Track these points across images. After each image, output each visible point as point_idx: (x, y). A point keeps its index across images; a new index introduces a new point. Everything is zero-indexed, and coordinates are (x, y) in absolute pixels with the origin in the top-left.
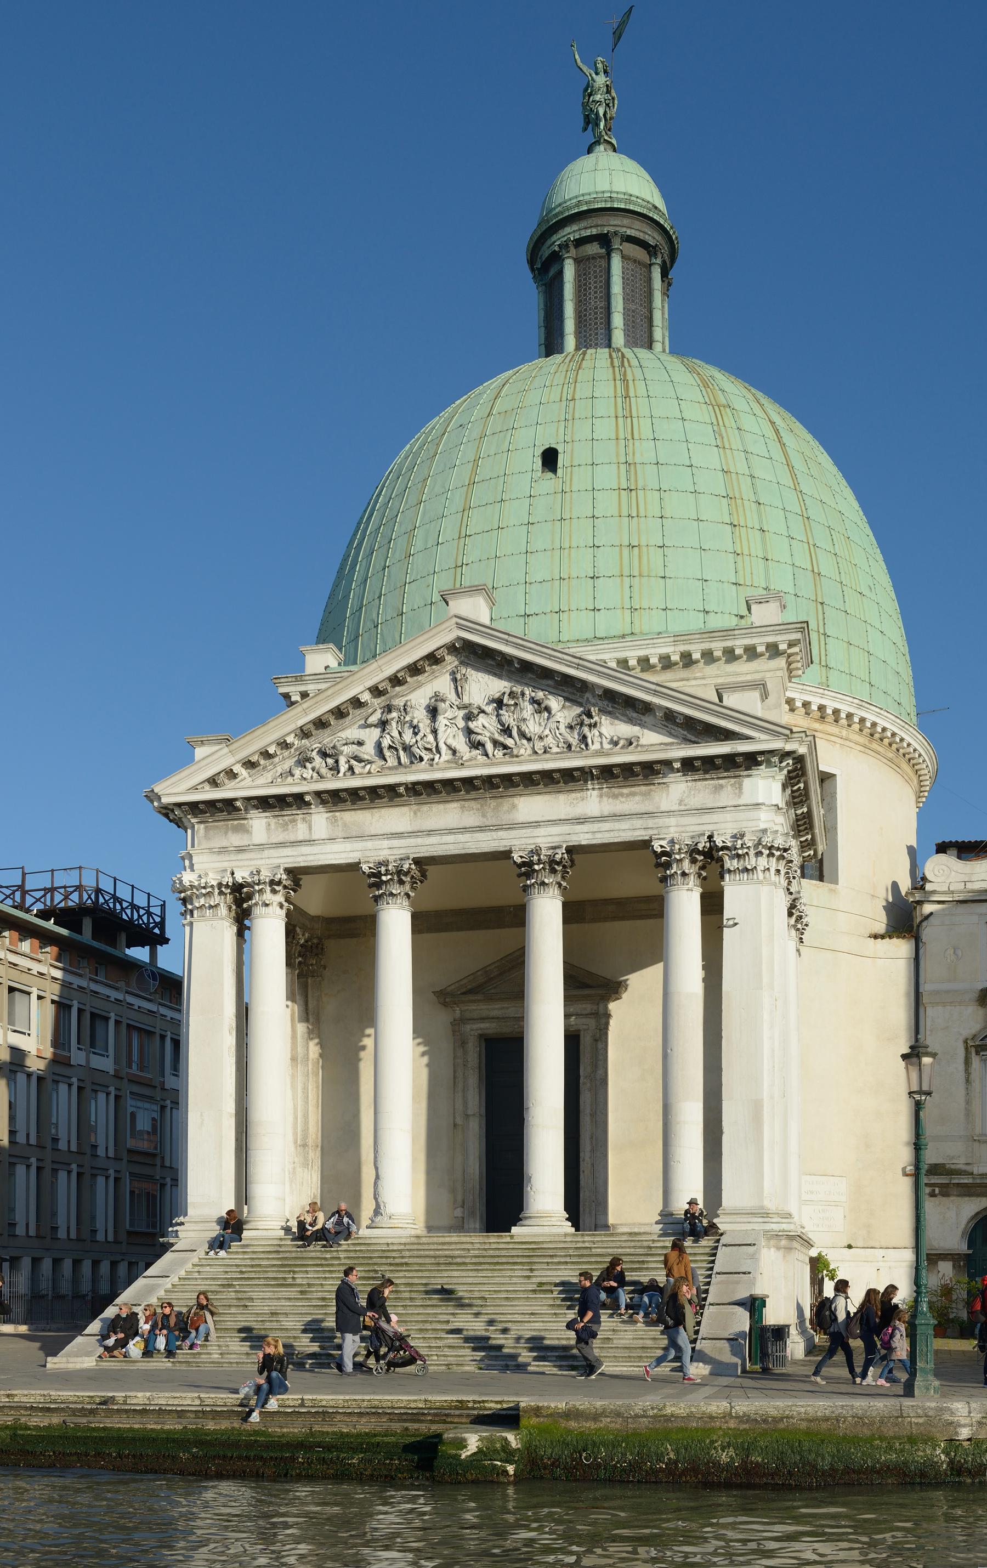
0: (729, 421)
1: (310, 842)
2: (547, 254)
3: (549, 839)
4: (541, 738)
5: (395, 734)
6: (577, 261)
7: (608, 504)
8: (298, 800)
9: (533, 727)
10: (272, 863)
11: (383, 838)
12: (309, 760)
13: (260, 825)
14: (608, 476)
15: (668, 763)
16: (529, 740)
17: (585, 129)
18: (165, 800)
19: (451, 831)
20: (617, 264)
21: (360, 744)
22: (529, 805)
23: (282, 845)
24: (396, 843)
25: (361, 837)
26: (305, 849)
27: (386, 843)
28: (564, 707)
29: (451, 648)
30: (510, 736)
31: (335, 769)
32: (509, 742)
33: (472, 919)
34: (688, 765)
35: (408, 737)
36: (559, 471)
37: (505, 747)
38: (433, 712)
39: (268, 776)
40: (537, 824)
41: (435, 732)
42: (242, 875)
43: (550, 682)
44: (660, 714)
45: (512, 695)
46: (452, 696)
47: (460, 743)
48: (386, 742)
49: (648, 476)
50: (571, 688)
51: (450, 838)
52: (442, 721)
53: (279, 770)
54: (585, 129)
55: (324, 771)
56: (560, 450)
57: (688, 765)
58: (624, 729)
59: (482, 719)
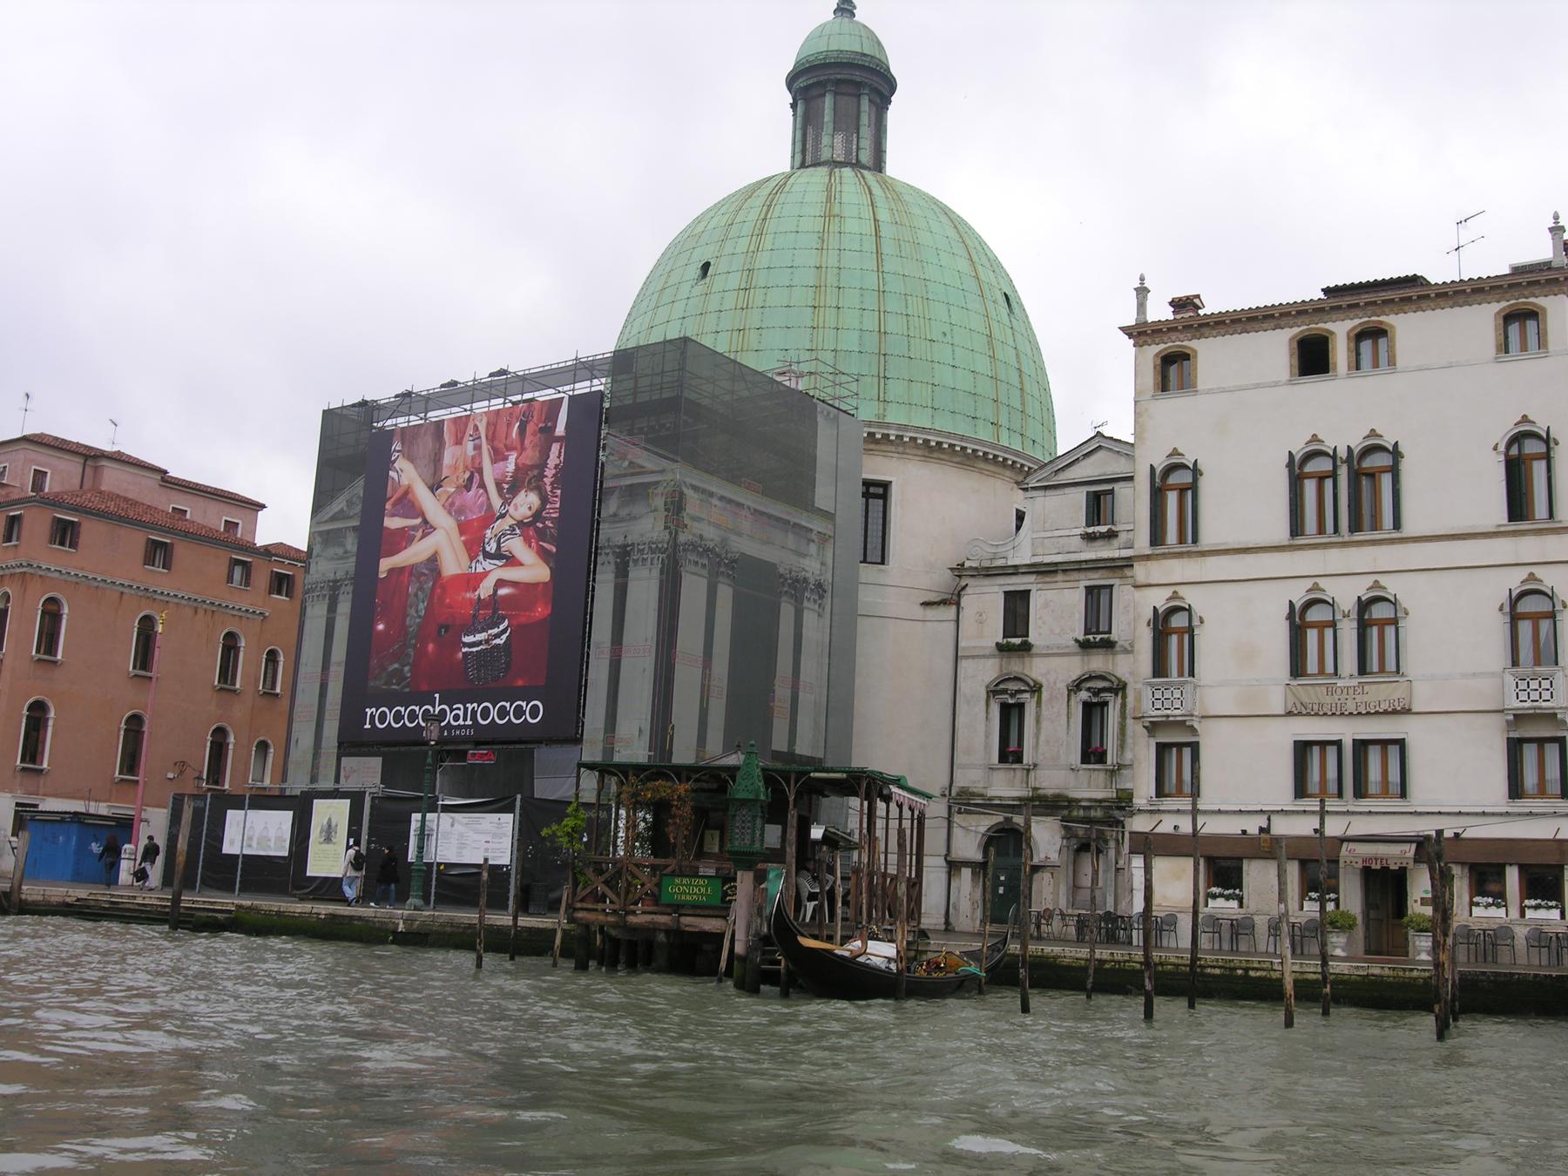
0: (834, 227)
6: (807, 101)
7: (730, 301)
14: (734, 281)
20: (828, 101)
49: (760, 279)
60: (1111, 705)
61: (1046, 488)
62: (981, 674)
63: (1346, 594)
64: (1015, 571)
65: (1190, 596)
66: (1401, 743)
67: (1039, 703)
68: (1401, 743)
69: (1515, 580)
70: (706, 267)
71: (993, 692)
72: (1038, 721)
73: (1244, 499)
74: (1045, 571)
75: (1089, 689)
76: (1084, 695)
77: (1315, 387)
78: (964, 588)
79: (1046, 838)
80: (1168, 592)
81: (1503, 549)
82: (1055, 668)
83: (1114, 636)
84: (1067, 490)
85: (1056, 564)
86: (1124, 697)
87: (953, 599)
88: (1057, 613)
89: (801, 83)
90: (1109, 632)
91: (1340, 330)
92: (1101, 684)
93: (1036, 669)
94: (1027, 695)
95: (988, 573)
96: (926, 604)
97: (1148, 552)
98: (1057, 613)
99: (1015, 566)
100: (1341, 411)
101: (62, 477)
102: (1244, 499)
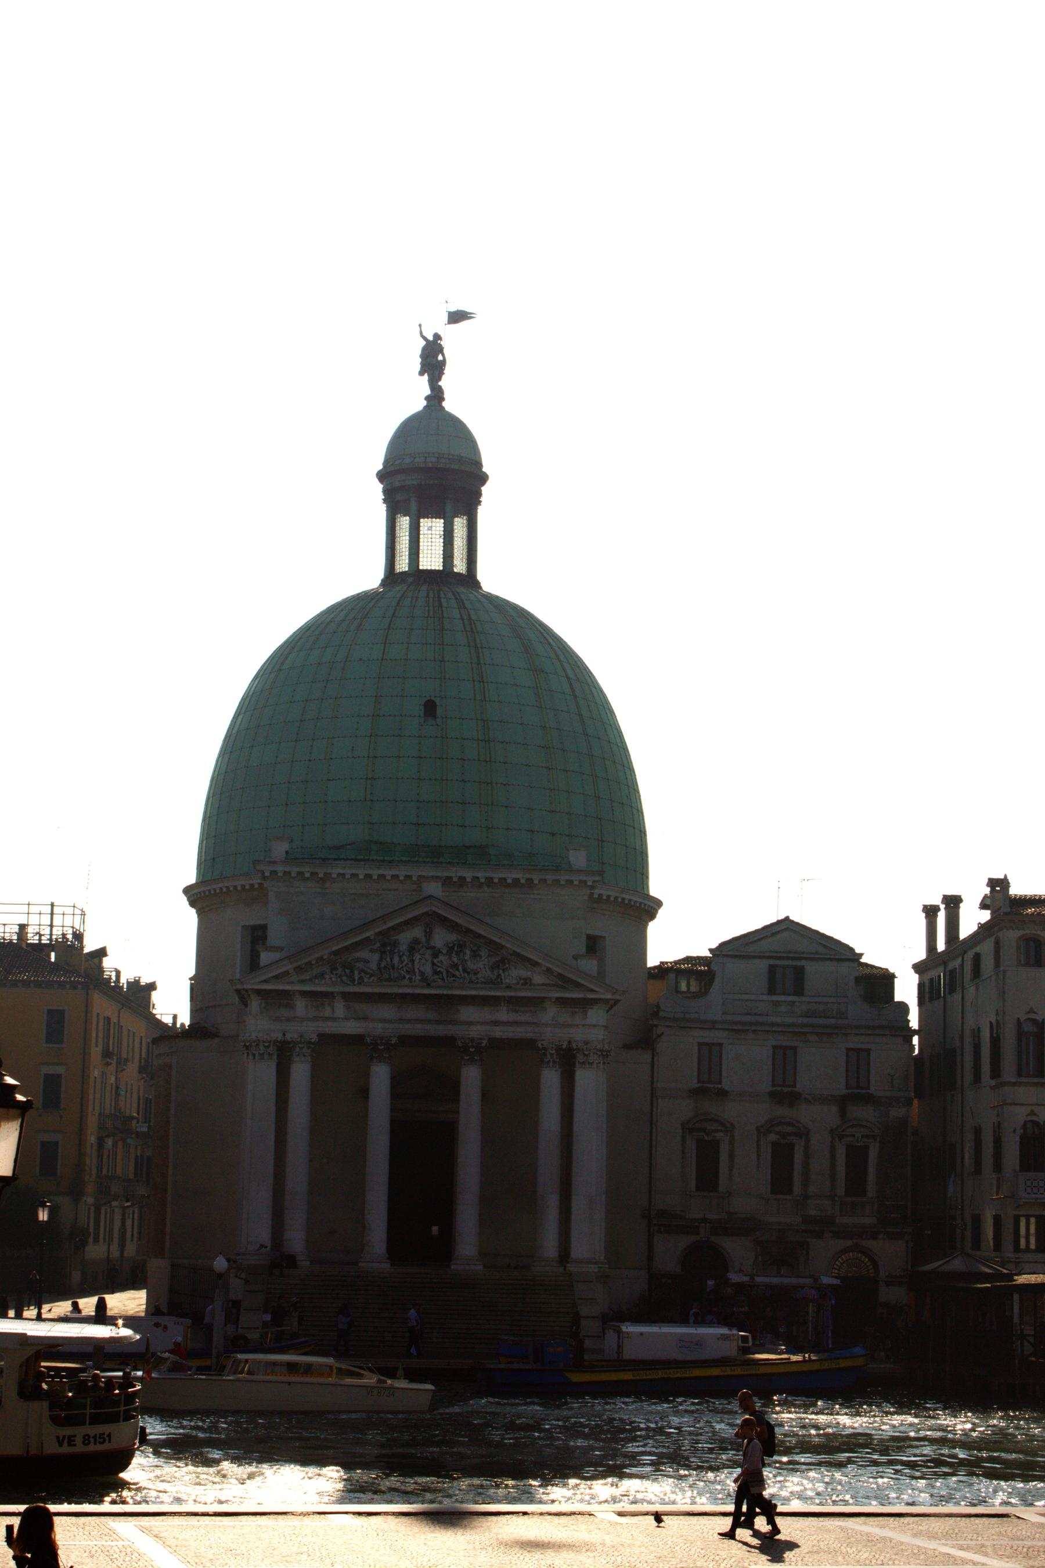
1: (333, 1019)
2: (397, 484)
3: (475, 1032)
4: (475, 974)
5: (388, 959)
8: (330, 995)
9: (470, 965)
10: (311, 1030)
11: (382, 1022)
12: (336, 969)
13: (301, 1006)
15: (550, 999)
16: (468, 973)
17: (421, 373)
18: (245, 987)
19: (420, 1021)
21: (367, 961)
22: (467, 1013)
23: (315, 1019)
24: (387, 1025)
25: (365, 1019)
26: (330, 1024)
27: (380, 1025)
28: (489, 955)
29: (426, 913)
30: (458, 970)
31: (351, 978)
32: (457, 973)
34: (562, 1002)
35: (396, 960)
36: (439, 720)
37: (454, 976)
38: (413, 948)
39: (307, 976)
40: (471, 1023)
41: (413, 961)
42: (288, 1037)
43: (482, 940)
44: (544, 968)
45: (460, 946)
46: (424, 940)
47: (428, 969)
48: (382, 966)
50: (495, 947)
51: (419, 1026)
52: (417, 957)
53: (315, 973)
54: (421, 373)
55: (344, 978)
56: (438, 701)
57: (562, 1002)
58: (522, 973)
59: (441, 957)
60: (796, 1148)
61: (736, 956)
64: (713, 1025)
67: (732, 1143)
70: (430, 708)
71: (688, 1128)
72: (731, 1156)
75: (778, 1133)
76: (773, 1137)
78: (660, 1036)
79: (739, 1251)
80: (1028, 1109)
83: (799, 1088)
84: (757, 961)
85: (751, 1024)
86: (807, 1141)
88: (747, 1064)
90: (794, 1086)
92: (788, 1129)
94: (720, 1135)
96: (628, 1047)
97: (1013, 1080)
98: (747, 1064)
99: (714, 1022)
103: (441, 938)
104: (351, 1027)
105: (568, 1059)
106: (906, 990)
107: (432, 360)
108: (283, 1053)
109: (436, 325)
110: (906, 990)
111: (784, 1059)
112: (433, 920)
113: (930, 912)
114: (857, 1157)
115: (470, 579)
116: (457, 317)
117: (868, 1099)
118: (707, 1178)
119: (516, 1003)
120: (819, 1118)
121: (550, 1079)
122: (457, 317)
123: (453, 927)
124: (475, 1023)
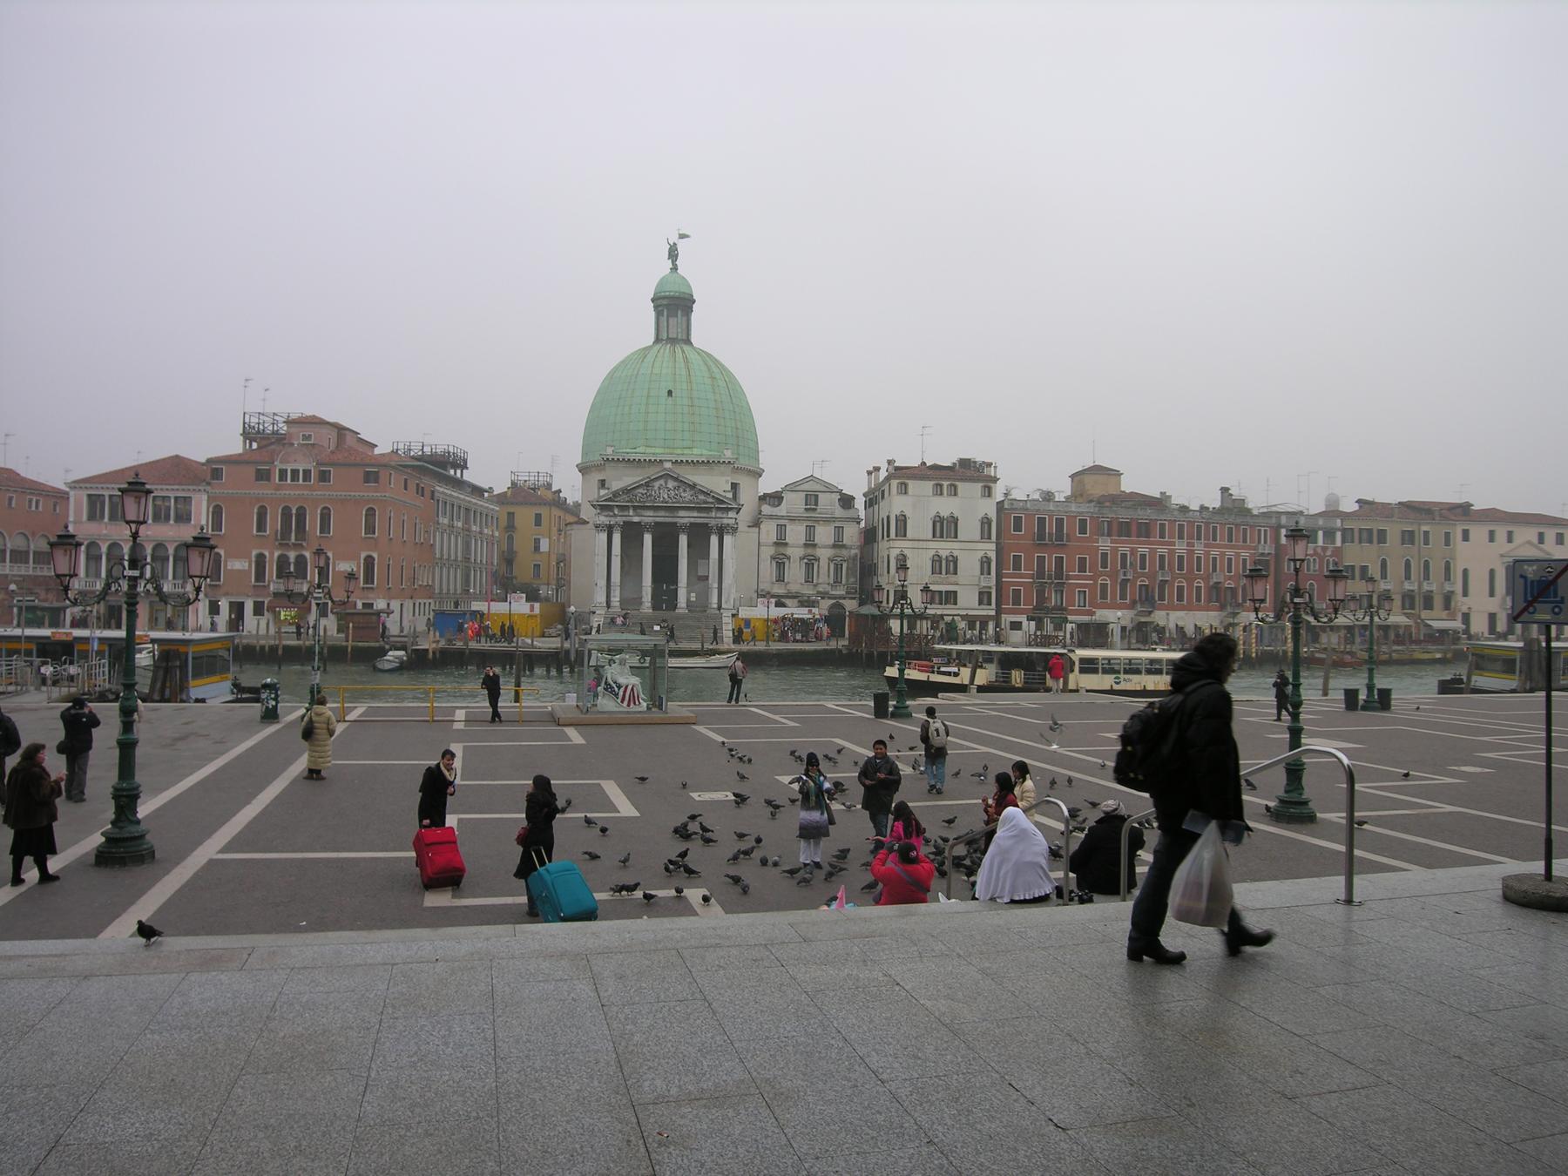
7: (686, 410)
10: (620, 520)
22: (682, 513)
33: (666, 538)
62: (767, 552)
63: (944, 554)
64: (782, 517)
65: (906, 552)
66: (955, 593)
68: (955, 593)
69: (981, 554)
70: (670, 393)
71: (773, 558)
73: (919, 526)
74: (792, 519)
77: (938, 499)
81: (980, 546)
82: (795, 552)
87: (756, 524)
88: (796, 534)
89: (665, 302)
91: (945, 484)
93: (789, 551)
95: (771, 517)
98: (796, 534)
100: (945, 506)
101: (328, 439)
102: (919, 526)
103: (671, 484)
104: (636, 519)
105: (721, 531)
106: (860, 503)
107: (673, 254)
108: (610, 530)
109: (674, 239)
110: (860, 503)
111: (810, 531)
112: (667, 476)
113: (869, 473)
114: (838, 568)
115: (688, 341)
116: (682, 236)
117: (844, 546)
118: (780, 579)
119: (700, 509)
120: (824, 554)
121: (714, 540)
122: (682, 236)
123: (676, 479)
124: (685, 518)
